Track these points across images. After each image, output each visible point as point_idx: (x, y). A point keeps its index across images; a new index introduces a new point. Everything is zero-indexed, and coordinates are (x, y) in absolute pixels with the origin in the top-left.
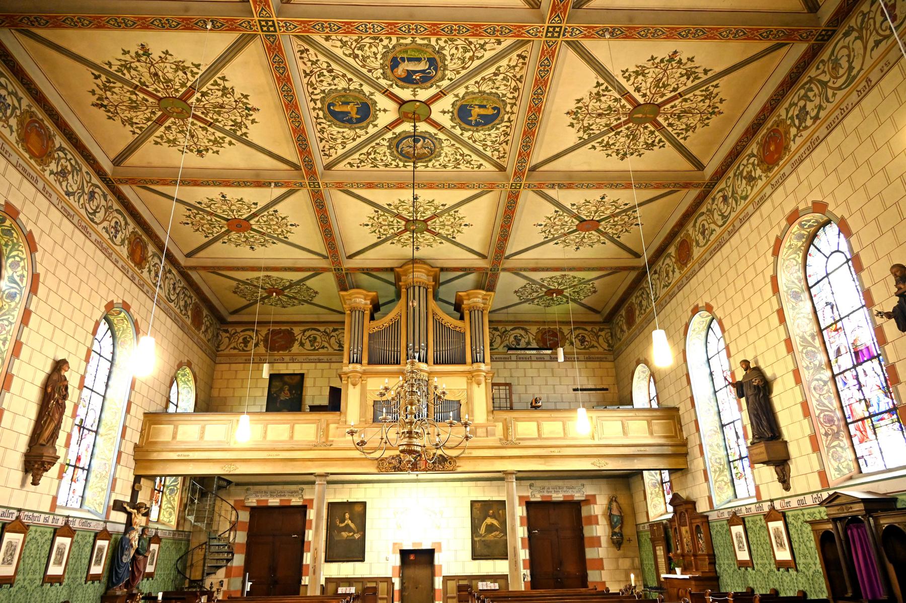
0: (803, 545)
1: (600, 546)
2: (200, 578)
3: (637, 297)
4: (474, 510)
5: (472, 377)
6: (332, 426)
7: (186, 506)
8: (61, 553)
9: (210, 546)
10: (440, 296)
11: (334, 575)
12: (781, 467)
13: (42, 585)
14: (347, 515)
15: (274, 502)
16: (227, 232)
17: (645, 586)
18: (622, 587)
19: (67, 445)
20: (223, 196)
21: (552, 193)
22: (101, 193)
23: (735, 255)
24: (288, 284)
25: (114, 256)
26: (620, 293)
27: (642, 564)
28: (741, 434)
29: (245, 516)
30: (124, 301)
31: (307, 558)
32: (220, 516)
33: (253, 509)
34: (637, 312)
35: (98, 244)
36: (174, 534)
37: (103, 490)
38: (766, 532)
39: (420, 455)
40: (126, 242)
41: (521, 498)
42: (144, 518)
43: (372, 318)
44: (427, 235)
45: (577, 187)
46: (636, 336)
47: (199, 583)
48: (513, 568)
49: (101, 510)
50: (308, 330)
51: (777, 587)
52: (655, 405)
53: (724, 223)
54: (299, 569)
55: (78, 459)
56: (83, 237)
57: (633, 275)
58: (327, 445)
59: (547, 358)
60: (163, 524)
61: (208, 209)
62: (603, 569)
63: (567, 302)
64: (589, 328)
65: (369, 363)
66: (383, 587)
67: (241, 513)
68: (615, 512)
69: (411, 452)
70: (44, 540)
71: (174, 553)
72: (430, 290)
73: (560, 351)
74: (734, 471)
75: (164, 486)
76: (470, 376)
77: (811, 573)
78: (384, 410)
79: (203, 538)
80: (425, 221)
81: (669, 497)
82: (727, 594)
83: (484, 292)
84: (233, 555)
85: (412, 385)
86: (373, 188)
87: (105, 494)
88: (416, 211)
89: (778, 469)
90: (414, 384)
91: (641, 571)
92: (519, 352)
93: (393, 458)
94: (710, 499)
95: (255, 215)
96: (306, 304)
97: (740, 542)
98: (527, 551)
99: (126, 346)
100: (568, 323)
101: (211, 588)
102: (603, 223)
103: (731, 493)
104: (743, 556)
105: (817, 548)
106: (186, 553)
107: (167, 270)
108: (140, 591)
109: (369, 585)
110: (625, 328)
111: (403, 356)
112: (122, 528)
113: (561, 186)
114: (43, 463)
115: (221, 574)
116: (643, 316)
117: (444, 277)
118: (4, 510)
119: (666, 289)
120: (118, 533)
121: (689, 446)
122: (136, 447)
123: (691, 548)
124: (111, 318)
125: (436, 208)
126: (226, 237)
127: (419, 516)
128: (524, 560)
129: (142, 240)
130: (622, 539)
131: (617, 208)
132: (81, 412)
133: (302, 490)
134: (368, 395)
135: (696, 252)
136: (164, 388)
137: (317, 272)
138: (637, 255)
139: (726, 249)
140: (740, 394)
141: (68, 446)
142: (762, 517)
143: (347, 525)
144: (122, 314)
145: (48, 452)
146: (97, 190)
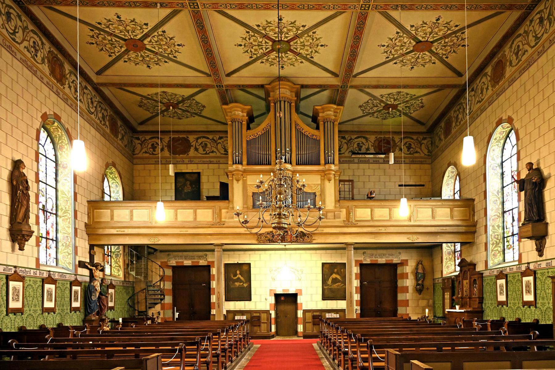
0: (543, 292)
1: (408, 292)
2: (145, 310)
3: (455, 111)
4: (324, 269)
5: (324, 175)
6: (224, 211)
7: (128, 265)
8: (50, 294)
9: (148, 291)
10: (301, 110)
11: (232, 308)
12: (540, 241)
13: (42, 314)
14: (238, 272)
15: (188, 263)
16: (127, 52)
17: (435, 316)
18: (420, 317)
19: (38, 223)
20: (118, 17)
21: (394, 14)
22: (15, 14)
23: (539, 74)
24: (181, 99)
25: (39, 73)
26: (442, 108)
27: (434, 303)
28: (516, 218)
29: (169, 272)
30: (54, 113)
31: (213, 299)
32: (152, 272)
33: (174, 268)
34: (454, 124)
35: (23, 62)
36: (123, 283)
37: (69, 254)
38: (520, 284)
39: (287, 232)
40: (46, 60)
41: (356, 261)
42: (101, 273)
43: (249, 128)
44: (290, 55)
45: (417, 9)
46: (451, 143)
47: (145, 313)
48: (349, 305)
49: (71, 267)
50: (200, 138)
51: (521, 317)
52: (457, 197)
53: (536, 44)
54: (209, 306)
55: (48, 233)
56: (11, 56)
57: (454, 92)
58: (221, 224)
59: (381, 161)
60: (115, 277)
61: (107, 30)
62: (408, 306)
63: (400, 116)
64: (415, 137)
65: (248, 164)
66: (264, 316)
67: (166, 270)
68: (420, 271)
69: (280, 228)
70: (37, 286)
71: (125, 295)
72: (293, 104)
73: (392, 155)
74: (506, 244)
75: (111, 252)
76: (323, 174)
77: (545, 308)
78: (261, 198)
79: (143, 286)
80: (288, 42)
81: (458, 262)
82: (487, 321)
83: (335, 106)
84: (164, 296)
85: (280, 180)
86: (243, 9)
87: (71, 257)
88: (281, 32)
89: (538, 242)
90: (282, 179)
91: (433, 308)
92: (361, 156)
93: (268, 234)
94: (486, 262)
95: (146, 36)
96: (197, 117)
97: (502, 290)
98: (359, 295)
99: (64, 150)
100: (399, 133)
101: (153, 316)
102: (435, 44)
103: (501, 258)
104: (502, 298)
105: (552, 294)
106: (134, 295)
107: (83, 86)
108: (107, 317)
109: (255, 315)
110: (442, 137)
111: (273, 158)
112: (88, 279)
113: (404, 8)
114: (23, 236)
115: (158, 307)
116: (457, 128)
117: (304, 93)
118: (5, 267)
119: (479, 104)
120: (85, 282)
121: (478, 226)
122: (86, 225)
123: (468, 293)
124: (48, 127)
125: (298, 29)
126: (126, 57)
127: (286, 274)
128: (356, 301)
129: (58, 59)
130: (423, 288)
131: (449, 29)
132: (42, 199)
133: (206, 255)
134: (248, 188)
135: (509, 71)
136: (98, 183)
137: (203, 88)
138: (460, 74)
139: (533, 69)
140: (521, 189)
141: (40, 225)
142: (520, 274)
143: (239, 278)
144: (56, 124)
145: (25, 228)
146: (11, 11)
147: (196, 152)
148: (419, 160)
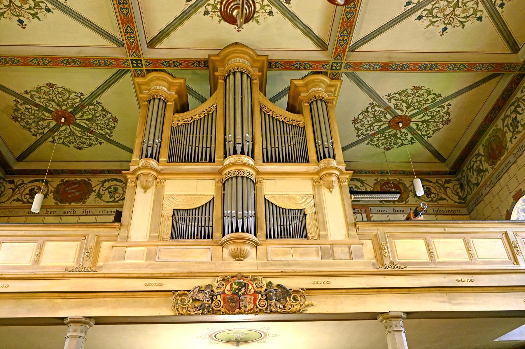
147: (98, 199)
148: (447, 209)
